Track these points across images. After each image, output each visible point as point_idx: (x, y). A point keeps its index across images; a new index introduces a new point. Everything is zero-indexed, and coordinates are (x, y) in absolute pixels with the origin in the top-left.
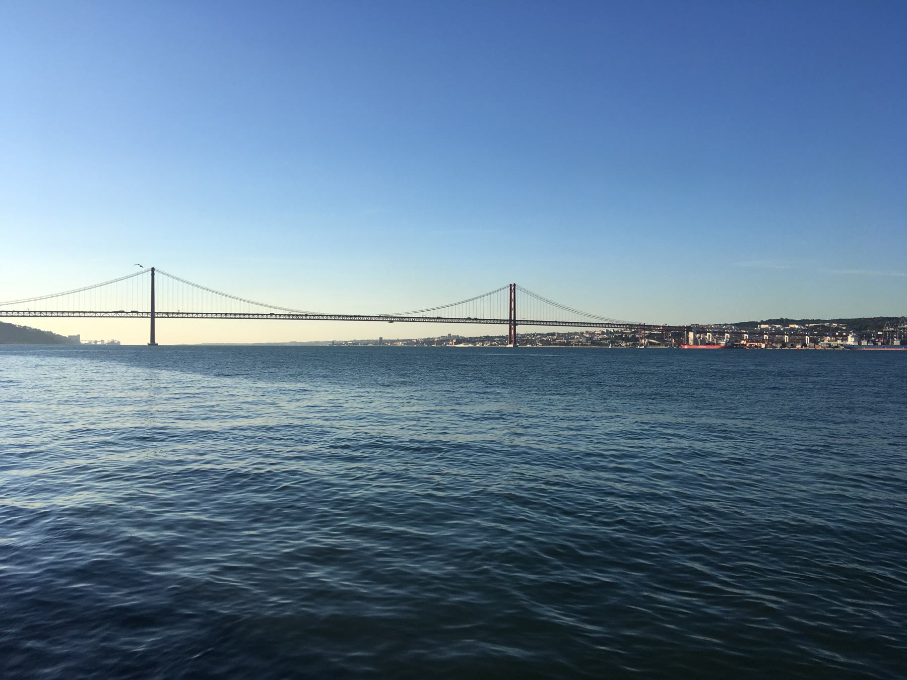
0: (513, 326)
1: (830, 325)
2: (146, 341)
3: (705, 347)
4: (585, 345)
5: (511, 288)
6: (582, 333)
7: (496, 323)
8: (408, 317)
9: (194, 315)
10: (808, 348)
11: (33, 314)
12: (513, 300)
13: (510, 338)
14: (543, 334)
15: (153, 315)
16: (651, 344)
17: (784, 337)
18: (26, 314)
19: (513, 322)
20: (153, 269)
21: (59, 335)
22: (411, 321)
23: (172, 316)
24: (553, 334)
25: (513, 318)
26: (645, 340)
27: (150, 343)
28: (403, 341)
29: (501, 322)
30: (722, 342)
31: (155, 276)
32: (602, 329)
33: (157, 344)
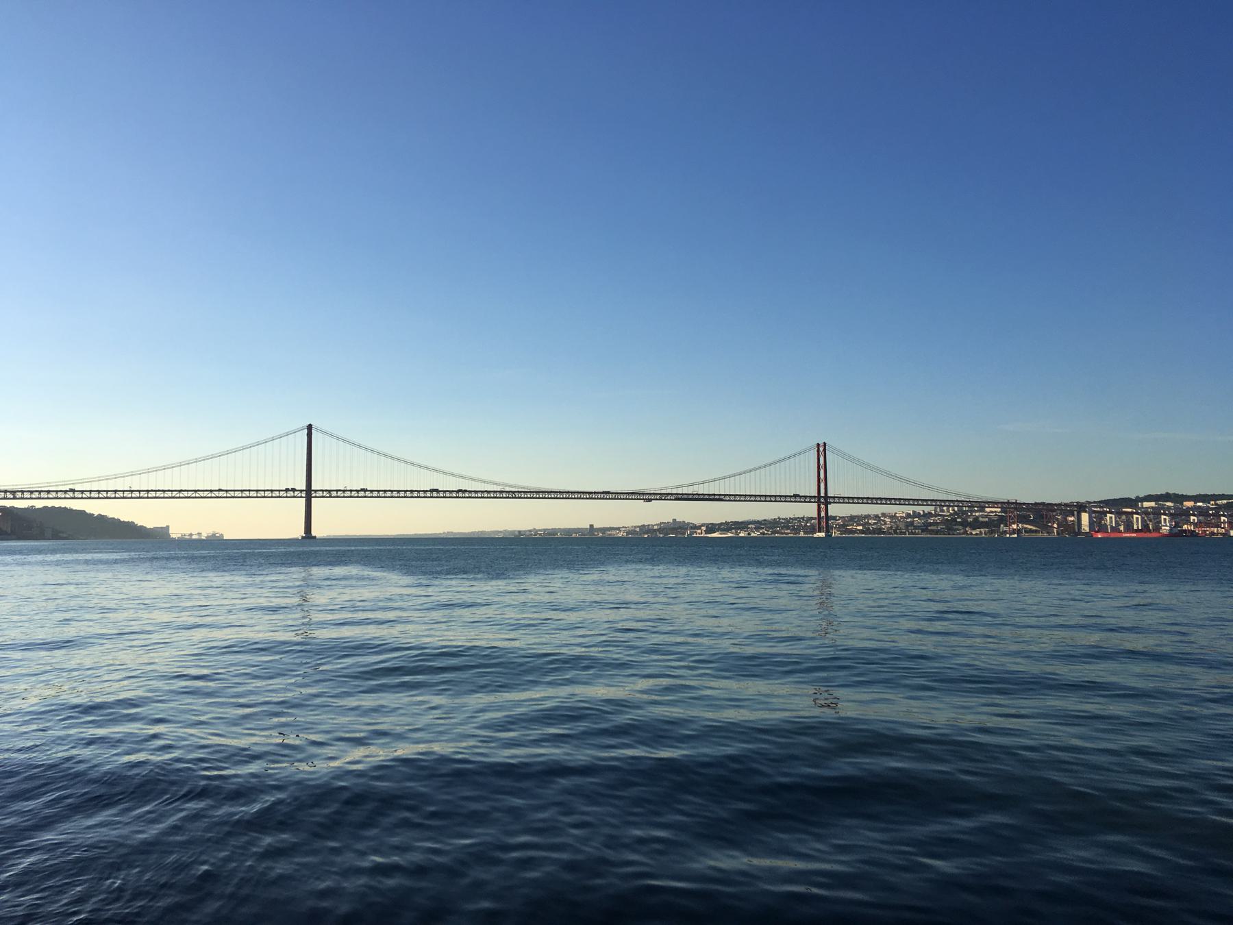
0: (822, 506)
2: (299, 532)
5: (818, 451)
6: (876, 517)
12: (822, 468)
15: (309, 493)
18: (126, 494)
20: (310, 427)
25: (822, 494)
26: (1018, 526)
27: (304, 535)
29: (805, 499)
30: (1163, 528)
31: (313, 436)
33: (315, 537)
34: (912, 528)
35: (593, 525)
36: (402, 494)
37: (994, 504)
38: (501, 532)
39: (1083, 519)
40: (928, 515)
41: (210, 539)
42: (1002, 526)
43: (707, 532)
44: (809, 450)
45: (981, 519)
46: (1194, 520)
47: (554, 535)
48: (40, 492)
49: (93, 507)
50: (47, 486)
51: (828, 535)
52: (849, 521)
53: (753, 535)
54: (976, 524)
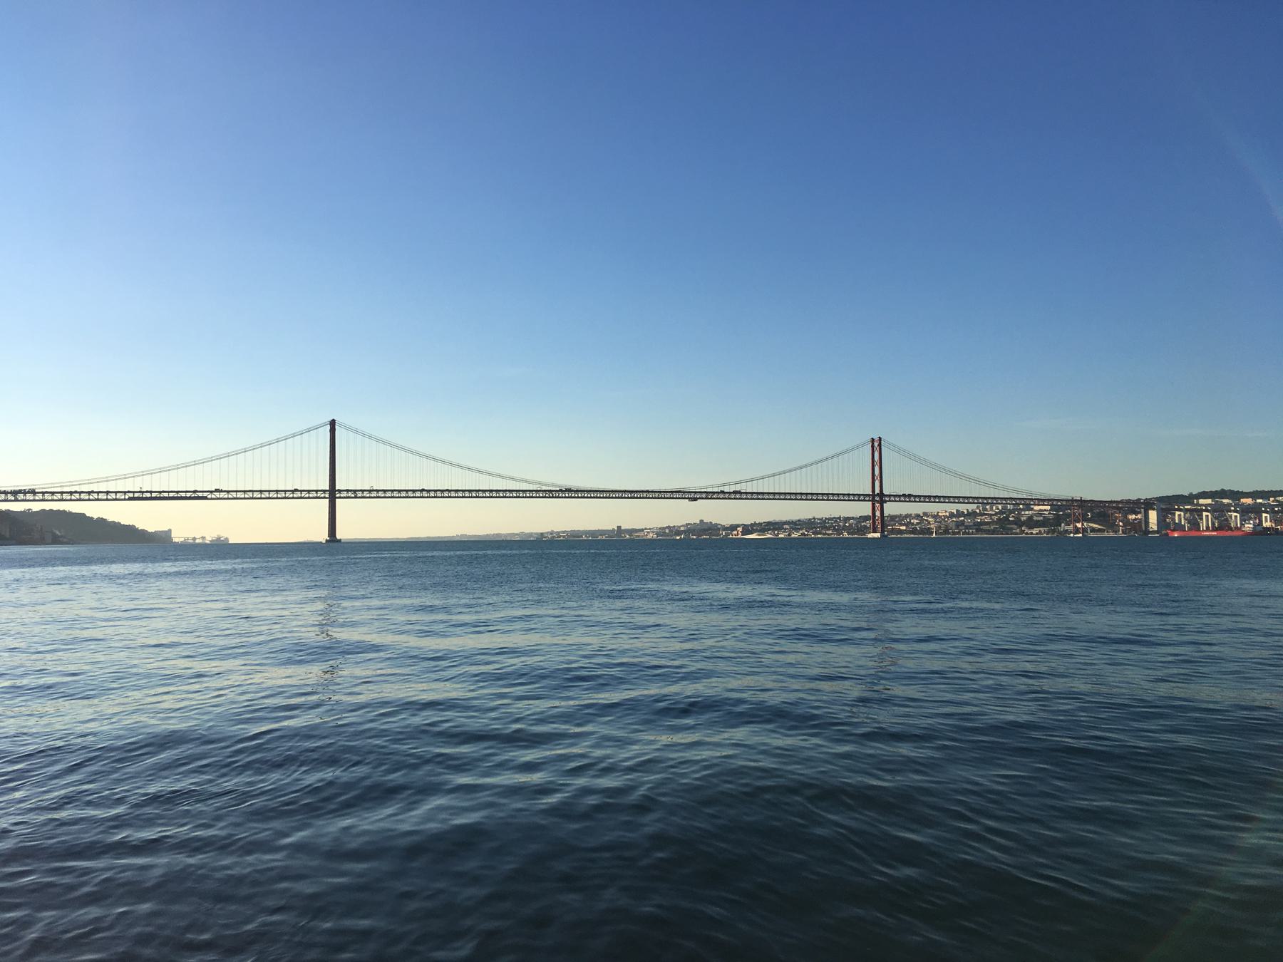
0: (877, 505)
2: (322, 536)
5: (873, 446)
6: (917, 516)
7: (723, 499)
12: (877, 464)
15: (332, 494)
16: (1093, 530)
19: (879, 498)
20: (333, 423)
25: (877, 491)
26: (1083, 524)
27: (328, 539)
29: (859, 497)
30: (1246, 525)
33: (340, 540)
34: (963, 527)
35: (620, 527)
36: (403, 494)
37: (1042, 501)
38: (517, 534)
39: (1150, 517)
40: (972, 514)
42: (1063, 525)
44: (863, 445)
45: (1035, 518)
47: (578, 537)
49: (93, 510)
50: (54, 487)
53: (793, 536)
54: (1031, 523)
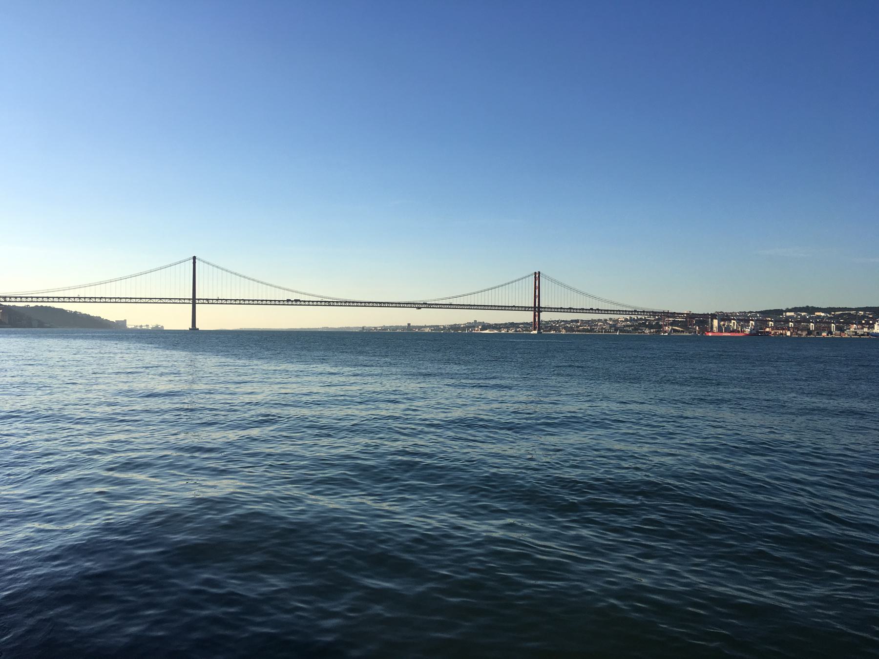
0: (537, 313)
1: (857, 313)
2: (188, 326)
3: (729, 334)
4: (608, 332)
5: (535, 276)
6: (606, 320)
8: (436, 304)
9: (232, 302)
10: (834, 336)
11: (83, 300)
12: (537, 288)
13: (535, 324)
14: (566, 321)
15: (194, 301)
16: (675, 331)
17: (810, 325)
19: (537, 309)
20: (194, 258)
21: (107, 320)
22: (438, 308)
23: (212, 302)
24: (577, 321)
25: (537, 306)
27: (191, 328)
28: (430, 327)
29: (526, 309)
30: (747, 330)
32: (626, 316)
33: (198, 329)
35: (410, 324)
41: (156, 329)
43: (481, 330)
46: (791, 325)
48: (21, 297)
51: (539, 332)
52: (585, 323)
53: (510, 332)
